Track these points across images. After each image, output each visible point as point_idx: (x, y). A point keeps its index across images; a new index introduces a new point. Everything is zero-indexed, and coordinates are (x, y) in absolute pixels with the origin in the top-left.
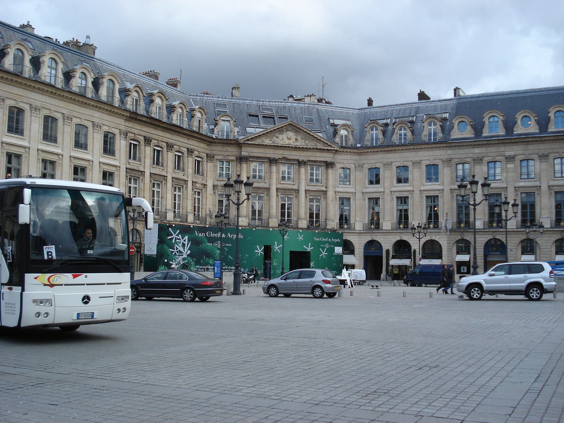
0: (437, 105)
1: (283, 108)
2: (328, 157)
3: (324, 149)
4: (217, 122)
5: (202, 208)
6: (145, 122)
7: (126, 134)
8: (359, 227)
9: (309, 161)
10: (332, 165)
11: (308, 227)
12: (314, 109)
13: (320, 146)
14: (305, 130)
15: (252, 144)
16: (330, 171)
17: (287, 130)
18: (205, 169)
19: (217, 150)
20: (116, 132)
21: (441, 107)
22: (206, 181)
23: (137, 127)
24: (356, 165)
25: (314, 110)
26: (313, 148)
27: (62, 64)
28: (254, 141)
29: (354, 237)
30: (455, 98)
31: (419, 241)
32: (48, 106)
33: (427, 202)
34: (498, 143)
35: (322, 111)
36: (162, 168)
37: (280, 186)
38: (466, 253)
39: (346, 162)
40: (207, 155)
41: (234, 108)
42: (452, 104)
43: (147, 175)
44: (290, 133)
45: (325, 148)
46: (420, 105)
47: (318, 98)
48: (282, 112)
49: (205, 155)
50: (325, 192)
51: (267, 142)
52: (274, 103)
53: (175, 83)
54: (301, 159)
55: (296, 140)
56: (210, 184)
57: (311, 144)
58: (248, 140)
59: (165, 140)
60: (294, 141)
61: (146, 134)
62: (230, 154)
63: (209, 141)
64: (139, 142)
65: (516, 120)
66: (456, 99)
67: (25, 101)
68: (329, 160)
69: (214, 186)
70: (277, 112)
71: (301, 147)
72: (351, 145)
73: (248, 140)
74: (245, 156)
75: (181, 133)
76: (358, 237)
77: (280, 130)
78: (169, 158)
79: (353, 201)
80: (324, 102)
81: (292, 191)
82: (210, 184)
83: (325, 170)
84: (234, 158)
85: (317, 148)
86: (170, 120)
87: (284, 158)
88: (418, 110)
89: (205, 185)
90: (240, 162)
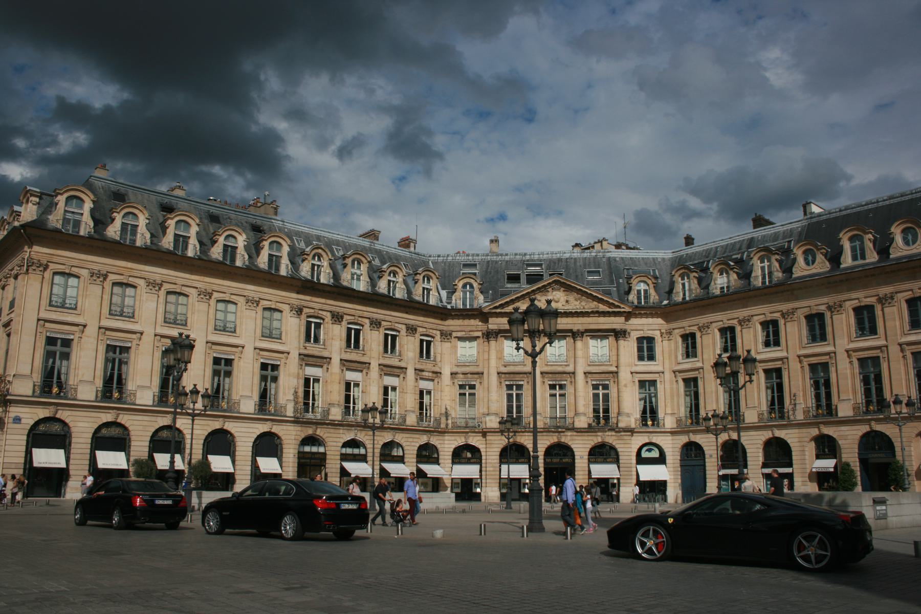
0: (779, 232)
1: (559, 261)
2: (616, 323)
3: (608, 312)
4: (456, 287)
5: (434, 405)
6: (329, 292)
7: (299, 311)
8: (669, 423)
9: (587, 331)
10: (625, 335)
11: (590, 425)
12: (604, 257)
13: (602, 308)
14: (579, 287)
15: (500, 313)
16: (621, 342)
17: (553, 289)
18: (439, 350)
19: (453, 324)
20: (285, 308)
21: (784, 233)
22: (440, 368)
24: (662, 331)
25: (604, 260)
26: (592, 312)
27: (197, 226)
28: (506, 308)
29: (663, 438)
30: (806, 217)
31: (717, 439)
32: (173, 280)
33: (767, 378)
34: (867, 276)
35: (615, 260)
36: (363, 352)
38: (831, 457)
39: (646, 328)
41: (488, 266)
42: (799, 227)
43: (336, 361)
44: (558, 293)
45: (610, 310)
46: (755, 235)
47: (615, 243)
48: (556, 267)
49: (438, 333)
50: (616, 374)
53: (407, 242)
54: (575, 328)
55: (567, 301)
57: (590, 306)
59: (366, 314)
60: (564, 303)
61: (333, 309)
62: (474, 328)
63: (442, 313)
64: (323, 320)
65: (892, 236)
66: (807, 219)
67: (136, 275)
68: (617, 327)
69: (453, 374)
70: (548, 268)
71: (573, 311)
72: (653, 303)
73: (496, 308)
74: (492, 330)
75: (392, 304)
76: (670, 438)
78: (372, 340)
79: (661, 384)
80: (623, 247)
81: (565, 375)
83: (615, 342)
84: (479, 334)
85: (597, 312)
86: (377, 288)
88: (751, 242)
90: (488, 339)
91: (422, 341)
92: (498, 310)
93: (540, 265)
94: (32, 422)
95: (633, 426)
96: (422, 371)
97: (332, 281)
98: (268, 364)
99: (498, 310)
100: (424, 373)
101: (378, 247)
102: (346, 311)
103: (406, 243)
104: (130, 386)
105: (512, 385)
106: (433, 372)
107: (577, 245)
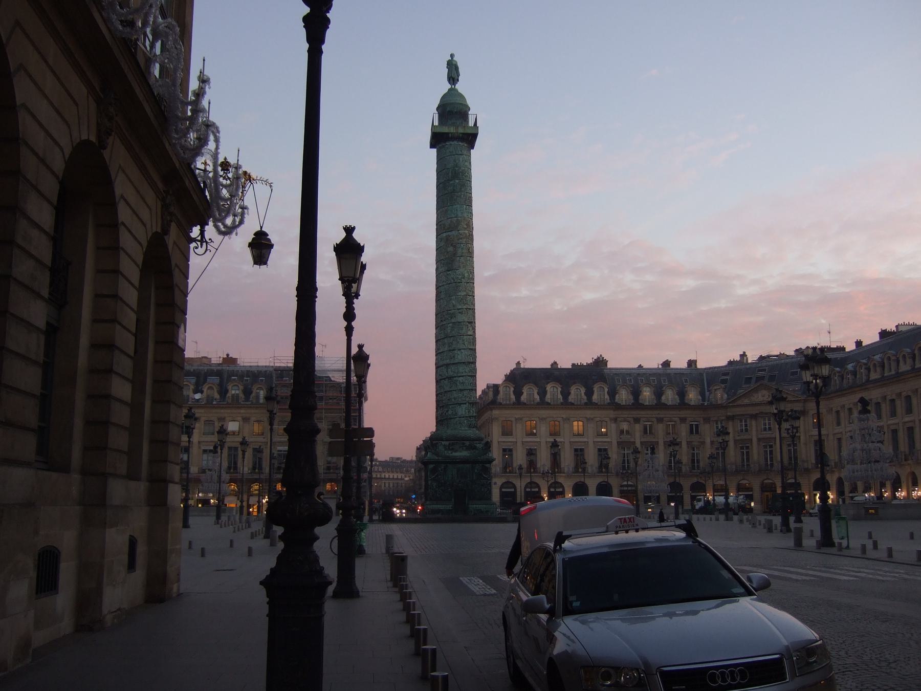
3: (791, 400)
20: (607, 419)
23: (626, 413)
37: (760, 436)
40: (704, 419)
51: (746, 401)
52: (770, 363)
56: (708, 441)
58: (730, 403)
61: (634, 416)
69: (712, 443)
73: (730, 403)
77: (756, 390)
82: (708, 441)
84: (723, 418)
87: (762, 413)
89: (703, 443)
91: (691, 426)
92: (731, 405)
93: (765, 370)
94: (500, 484)
95: (810, 467)
96: (692, 442)
97: (633, 401)
98: (601, 449)
99: (731, 405)
100: (693, 443)
101: (669, 371)
102: (640, 416)
103: (692, 363)
104: (538, 466)
105: (743, 447)
106: (699, 442)
107: (796, 351)
